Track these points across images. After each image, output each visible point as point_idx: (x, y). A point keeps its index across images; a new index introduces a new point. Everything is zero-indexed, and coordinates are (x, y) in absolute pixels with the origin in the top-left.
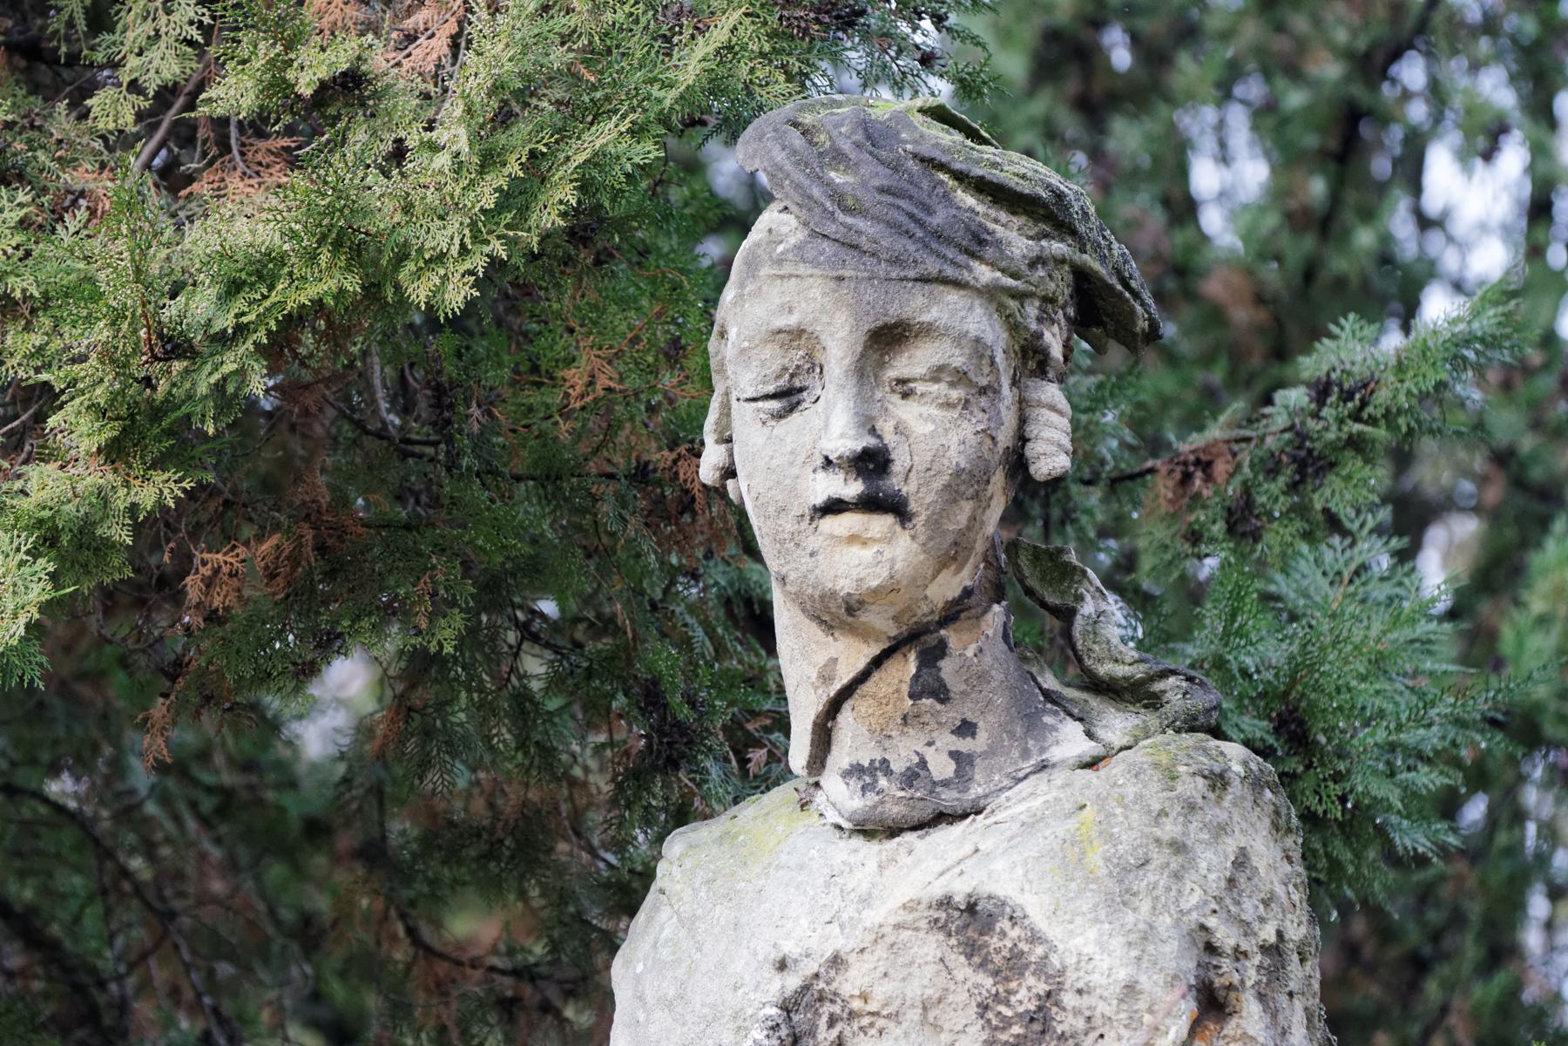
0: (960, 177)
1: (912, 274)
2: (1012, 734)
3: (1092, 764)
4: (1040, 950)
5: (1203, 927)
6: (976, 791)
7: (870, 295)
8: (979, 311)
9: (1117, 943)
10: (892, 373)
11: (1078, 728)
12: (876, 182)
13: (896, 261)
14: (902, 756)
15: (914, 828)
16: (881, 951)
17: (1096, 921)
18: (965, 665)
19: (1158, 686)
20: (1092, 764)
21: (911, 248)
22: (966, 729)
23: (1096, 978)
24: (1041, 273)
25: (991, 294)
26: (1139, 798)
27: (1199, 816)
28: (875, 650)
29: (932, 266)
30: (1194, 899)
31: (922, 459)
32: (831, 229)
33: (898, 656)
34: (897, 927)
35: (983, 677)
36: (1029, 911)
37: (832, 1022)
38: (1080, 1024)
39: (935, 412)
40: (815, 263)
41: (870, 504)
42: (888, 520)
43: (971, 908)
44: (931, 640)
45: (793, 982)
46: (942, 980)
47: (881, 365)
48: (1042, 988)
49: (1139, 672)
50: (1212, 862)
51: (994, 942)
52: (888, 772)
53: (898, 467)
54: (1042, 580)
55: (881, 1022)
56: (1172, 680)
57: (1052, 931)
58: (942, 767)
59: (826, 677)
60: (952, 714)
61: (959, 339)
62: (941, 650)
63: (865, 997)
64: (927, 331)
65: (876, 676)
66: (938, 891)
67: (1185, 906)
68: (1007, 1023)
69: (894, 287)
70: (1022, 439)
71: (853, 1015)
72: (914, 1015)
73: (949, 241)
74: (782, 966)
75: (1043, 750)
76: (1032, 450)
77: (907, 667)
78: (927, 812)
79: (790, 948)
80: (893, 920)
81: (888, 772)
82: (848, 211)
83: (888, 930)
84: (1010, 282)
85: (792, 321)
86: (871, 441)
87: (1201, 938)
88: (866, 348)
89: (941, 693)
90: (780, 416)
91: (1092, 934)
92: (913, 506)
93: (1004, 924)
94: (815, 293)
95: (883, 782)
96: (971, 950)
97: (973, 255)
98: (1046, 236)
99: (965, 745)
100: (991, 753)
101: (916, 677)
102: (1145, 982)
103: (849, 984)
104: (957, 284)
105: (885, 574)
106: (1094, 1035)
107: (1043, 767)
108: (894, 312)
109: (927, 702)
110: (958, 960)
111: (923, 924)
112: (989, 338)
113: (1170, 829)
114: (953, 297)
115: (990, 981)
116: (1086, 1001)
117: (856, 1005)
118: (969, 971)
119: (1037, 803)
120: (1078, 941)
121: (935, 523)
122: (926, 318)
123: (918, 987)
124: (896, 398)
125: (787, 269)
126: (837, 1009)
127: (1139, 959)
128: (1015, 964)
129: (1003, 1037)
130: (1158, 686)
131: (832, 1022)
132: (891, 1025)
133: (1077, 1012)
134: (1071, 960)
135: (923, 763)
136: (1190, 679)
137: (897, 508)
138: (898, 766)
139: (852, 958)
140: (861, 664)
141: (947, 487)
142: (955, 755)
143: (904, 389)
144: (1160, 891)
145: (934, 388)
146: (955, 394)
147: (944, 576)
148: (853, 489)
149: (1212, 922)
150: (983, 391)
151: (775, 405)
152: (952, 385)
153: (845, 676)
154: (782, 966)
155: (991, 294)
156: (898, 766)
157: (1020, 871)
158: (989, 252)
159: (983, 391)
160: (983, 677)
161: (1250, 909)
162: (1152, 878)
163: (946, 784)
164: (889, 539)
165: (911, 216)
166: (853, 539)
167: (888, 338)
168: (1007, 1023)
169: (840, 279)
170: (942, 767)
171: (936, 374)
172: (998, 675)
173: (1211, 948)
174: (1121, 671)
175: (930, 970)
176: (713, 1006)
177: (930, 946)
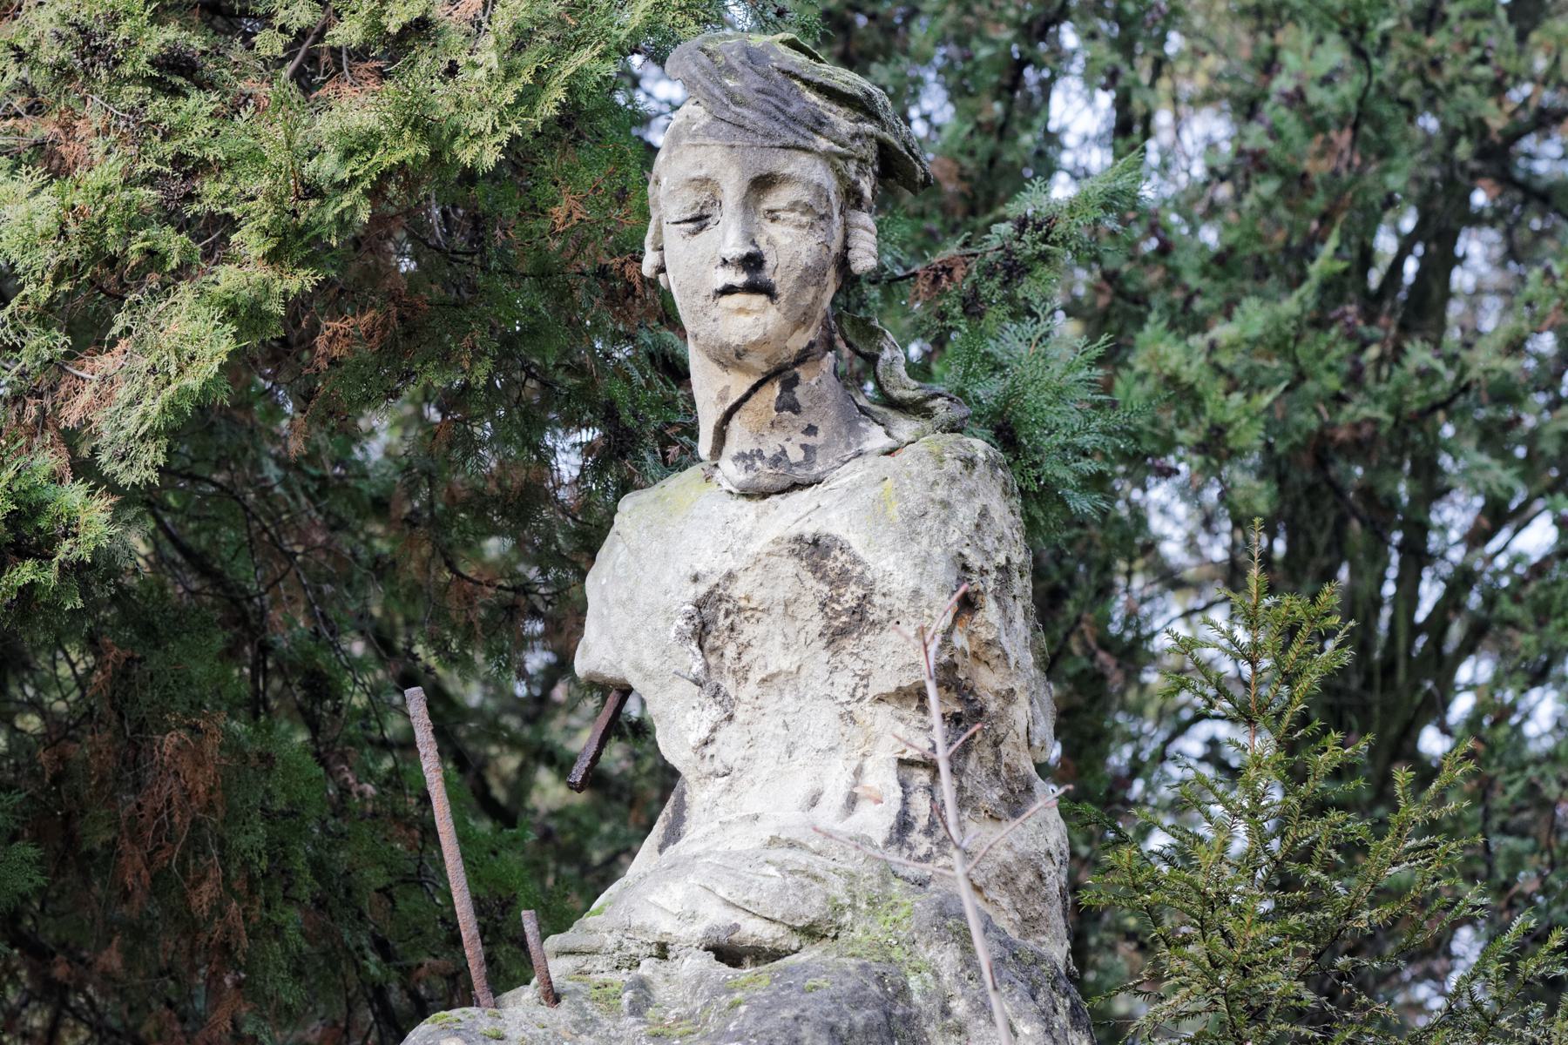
0: (807, 83)
1: (778, 143)
2: (839, 434)
3: (890, 452)
4: (859, 569)
5: (961, 555)
6: (817, 469)
7: (751, 156)
8: (819, 167)
9: (908, 564)
10: (765, 206)
11: (881, 430)
12: (755, 86)
13: (767, 135)
14: (770, 447)
15: (778, 493)
16: (758, 570)
17: (894, 550)
18: (810, 390)
19: (930, 404)
20: (890, 452)
21: (777, 127)
22: (811, 430)
23: (894, 586)
24: (858, 143)
25: (827, 156)
26: (920, 473)
27: (958, 485)
28: (754, 380)
29: (790, 139)
30: (955, 537)
31: (783, 261)
32: (726, 115)
33: (768, 385)
34: (769, 554)
35: (821, 398)
36: (853, 544)
37: (727, 615)
38: (885, 615)
39: (792, 230)
40: (716, 137)
41: (752, 288)
42: (763, 298)
43: (816, 543)
44: (789, 374)
45: (702, 589)
46: (797, 588)
47: (759, 201)
48: (860, 592)
49: (919, 395)
50: (966, 514)
51: (830, 563)
52: (762, 457)
53: (769, 265)
54: (857, 337)
55: (758, 615)
56: (939, 400)
57: (868, 557)
58: (795, 454)
59: (722, 398)
60: (802, 421)
61: (807, 185)
62: (795, 381)
63: (748, 599)
64: (787, 179)
65: (754, 397)
66: (794, 532)
67: (950, 541)
68: (838, 615)
69: (766, 152)
70: (846, 248)
71: (740, 610)
72: (780, 609)
73: (801, 123)
74: (696, 579)
75: (859, 444)
76: (852, 255)
77: (774, 391)
78: (787, 484)
79: (700, 568)
80: (766, 550)
81: (762, 457)
82: (737, 104)
83: (762, 556)
84: (839, 149)
85: (702, 173)
86: (752, 249)
87: (960, 561)
88: (749, 190)
89: (795, 408)
90: (694, 233)
91: (892, 559)
92: (778, 290)
93: (836, 552)
94: (717, 155)
95: (759, 464)
96: (815, 569)
97: (816, 132)
99: (810, 440)
100: (827, 445)
101: (779, 398)
102: (925, 589)
103: (738, 590)
104: (806, 150)
105: (761, 332)
106: (893, 622)
107: (859, 454)
108: (767, 167)
109: (787, 413)
110: (807, 575)
111: (785, 552)
112: (826, 184)
113: (940, 493)
114: (803, 158)
115: (827, 589)
116: (888, 600)
117: (743, 603)
118: (814, 582)
119: (856, 477)
120: (883, 563)
121: (792, 300)
122: (787, 171)
123: (783, 591)
124: (767, 222)
125: (699, 140)
126: (730, 606)
128: (843, 577)
129: (836, 623)
130: (930, 404)
131: (727, 615)
132: (765, 616)
133: (882, 607)
134: (879, 575)
135: (784, 452)
136: (951, 400)
137: (768, 291)
138: (768, 454)
139: (740, 574)
140: (745, 390)
142: (804, 447)
143: (773, 216)
144: (934, 532)
145: (792, 215)
146: (805, 219)
147: (798, 334)
148: (740, 279)
149: (966, 551)
150: (822, 217)
151: (691, 226)
152: (803, 213)
153: (734, 397)
154: (696, 579)
155: (827, 156)
156: (768, 454)
157: (846, 519)
158: (826, 130)
159: (822, 217)
160: (821, 398)
163: (798, 465)
164: (763, 311)
165: (777, 107)
166: (741, 310)
167: (762, 183)
168: (838, 615)
169: (732, 147)
170: (795, 454)
171: (793, 207)
172: (831, 397)
173: (965, 568)
174: (907, 394)
175: (789, 582)
176: (651, 605)
177: (789, 566)
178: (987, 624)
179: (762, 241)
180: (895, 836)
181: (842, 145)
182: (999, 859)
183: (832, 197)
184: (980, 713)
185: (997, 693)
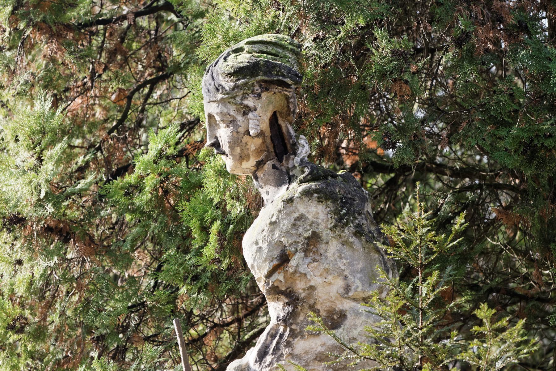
5: (280, 241)
24: (236, 90)
84: (227, 96)
98: (239, 80)
112: (225, 111)
127: (255, 258)
141: (229, 147)
159: (231, 122)
161: (301, 229)
162: (264, 234)
172: (271, 178)
173: (285, 246)
178: (292, 266)
179: (218, 135)
180: (258, 359)
181: (228, 94)
182: (317, 352)
183: (232, 113)
184: (298, 299)
185: (304, 289)
